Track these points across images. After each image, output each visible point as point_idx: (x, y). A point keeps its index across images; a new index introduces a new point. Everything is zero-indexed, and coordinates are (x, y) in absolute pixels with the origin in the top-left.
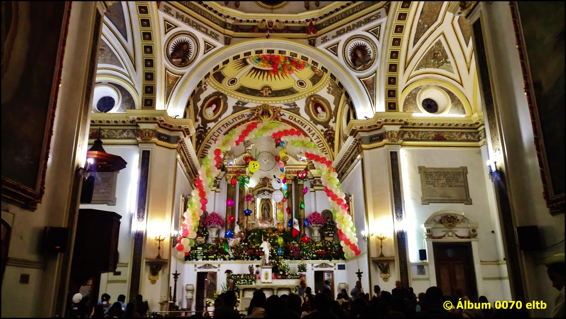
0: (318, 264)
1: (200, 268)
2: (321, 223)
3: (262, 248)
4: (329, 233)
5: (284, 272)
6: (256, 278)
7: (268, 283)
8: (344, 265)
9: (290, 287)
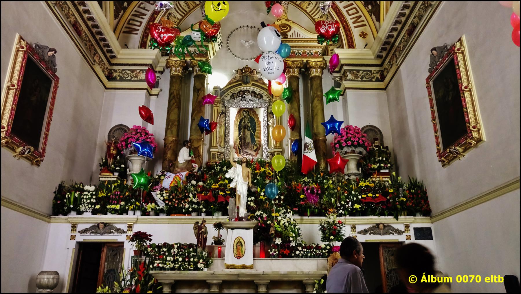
0: (367, 227)
1: (84, 232)
2: (363, 146)
3: (230, 180)
4: (380, 168)
5: (286, 241)
6: (210, 254)
7: (244, 267)
8: (429, 229)
9: (304, 279)
